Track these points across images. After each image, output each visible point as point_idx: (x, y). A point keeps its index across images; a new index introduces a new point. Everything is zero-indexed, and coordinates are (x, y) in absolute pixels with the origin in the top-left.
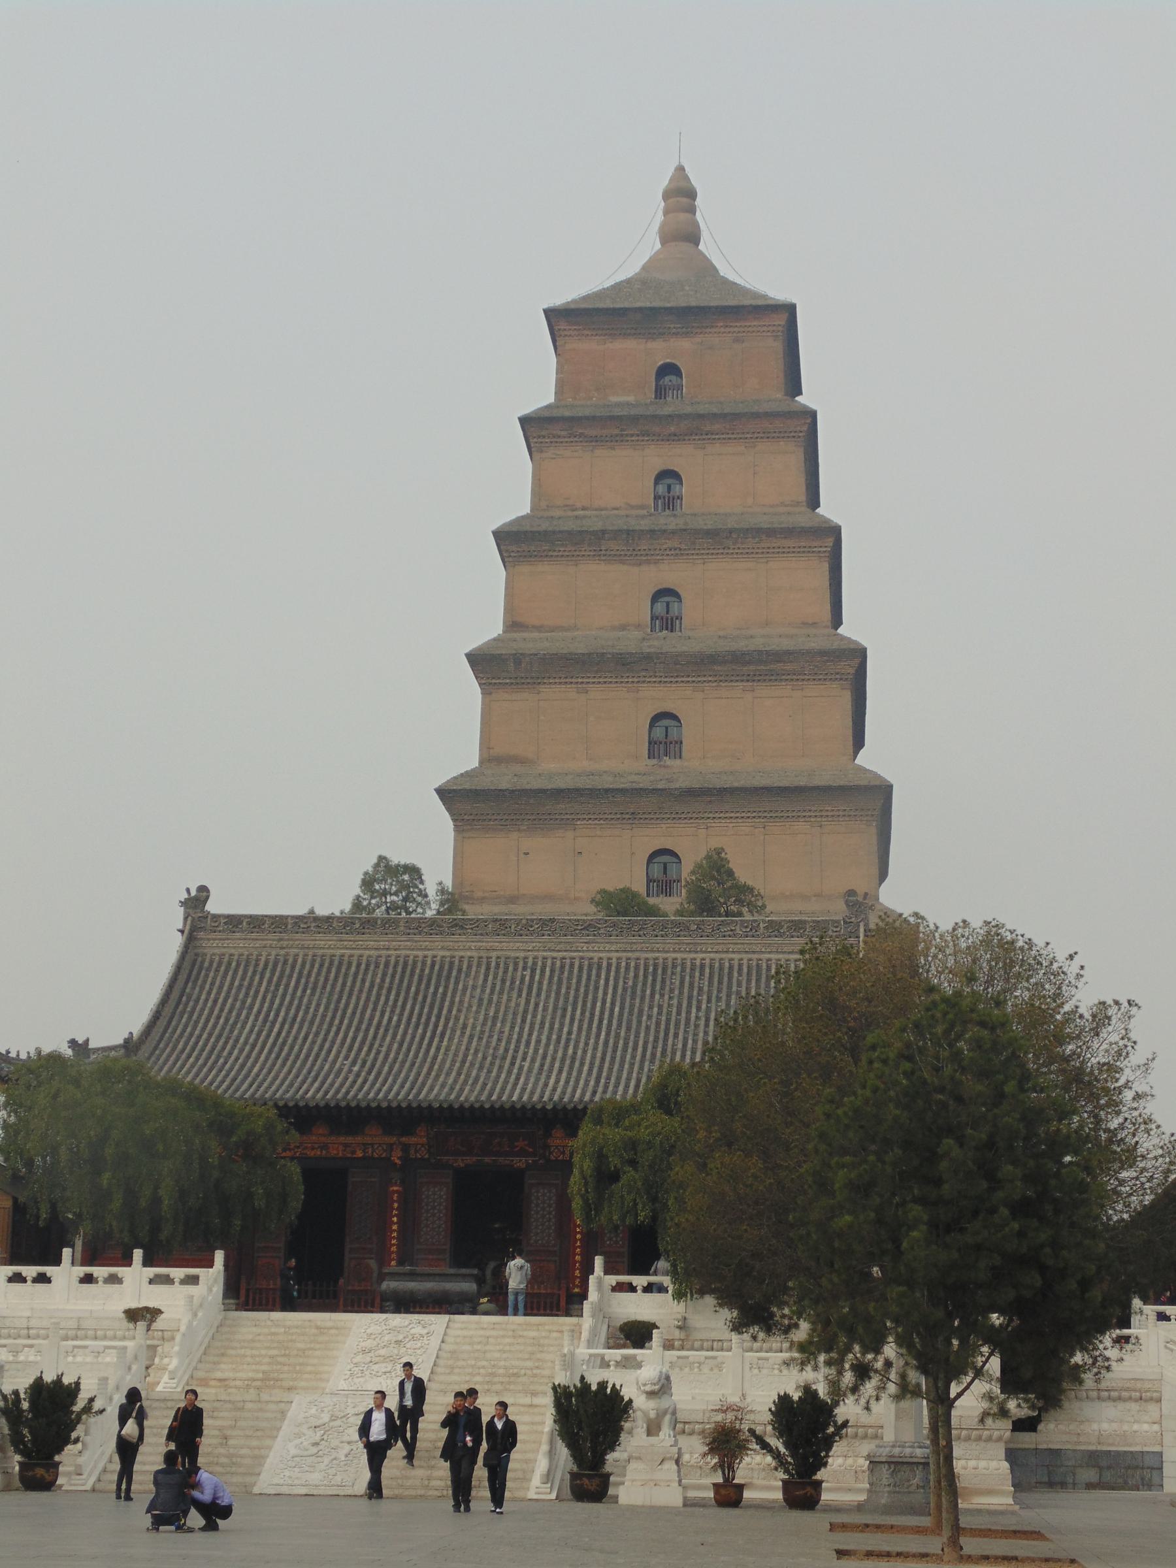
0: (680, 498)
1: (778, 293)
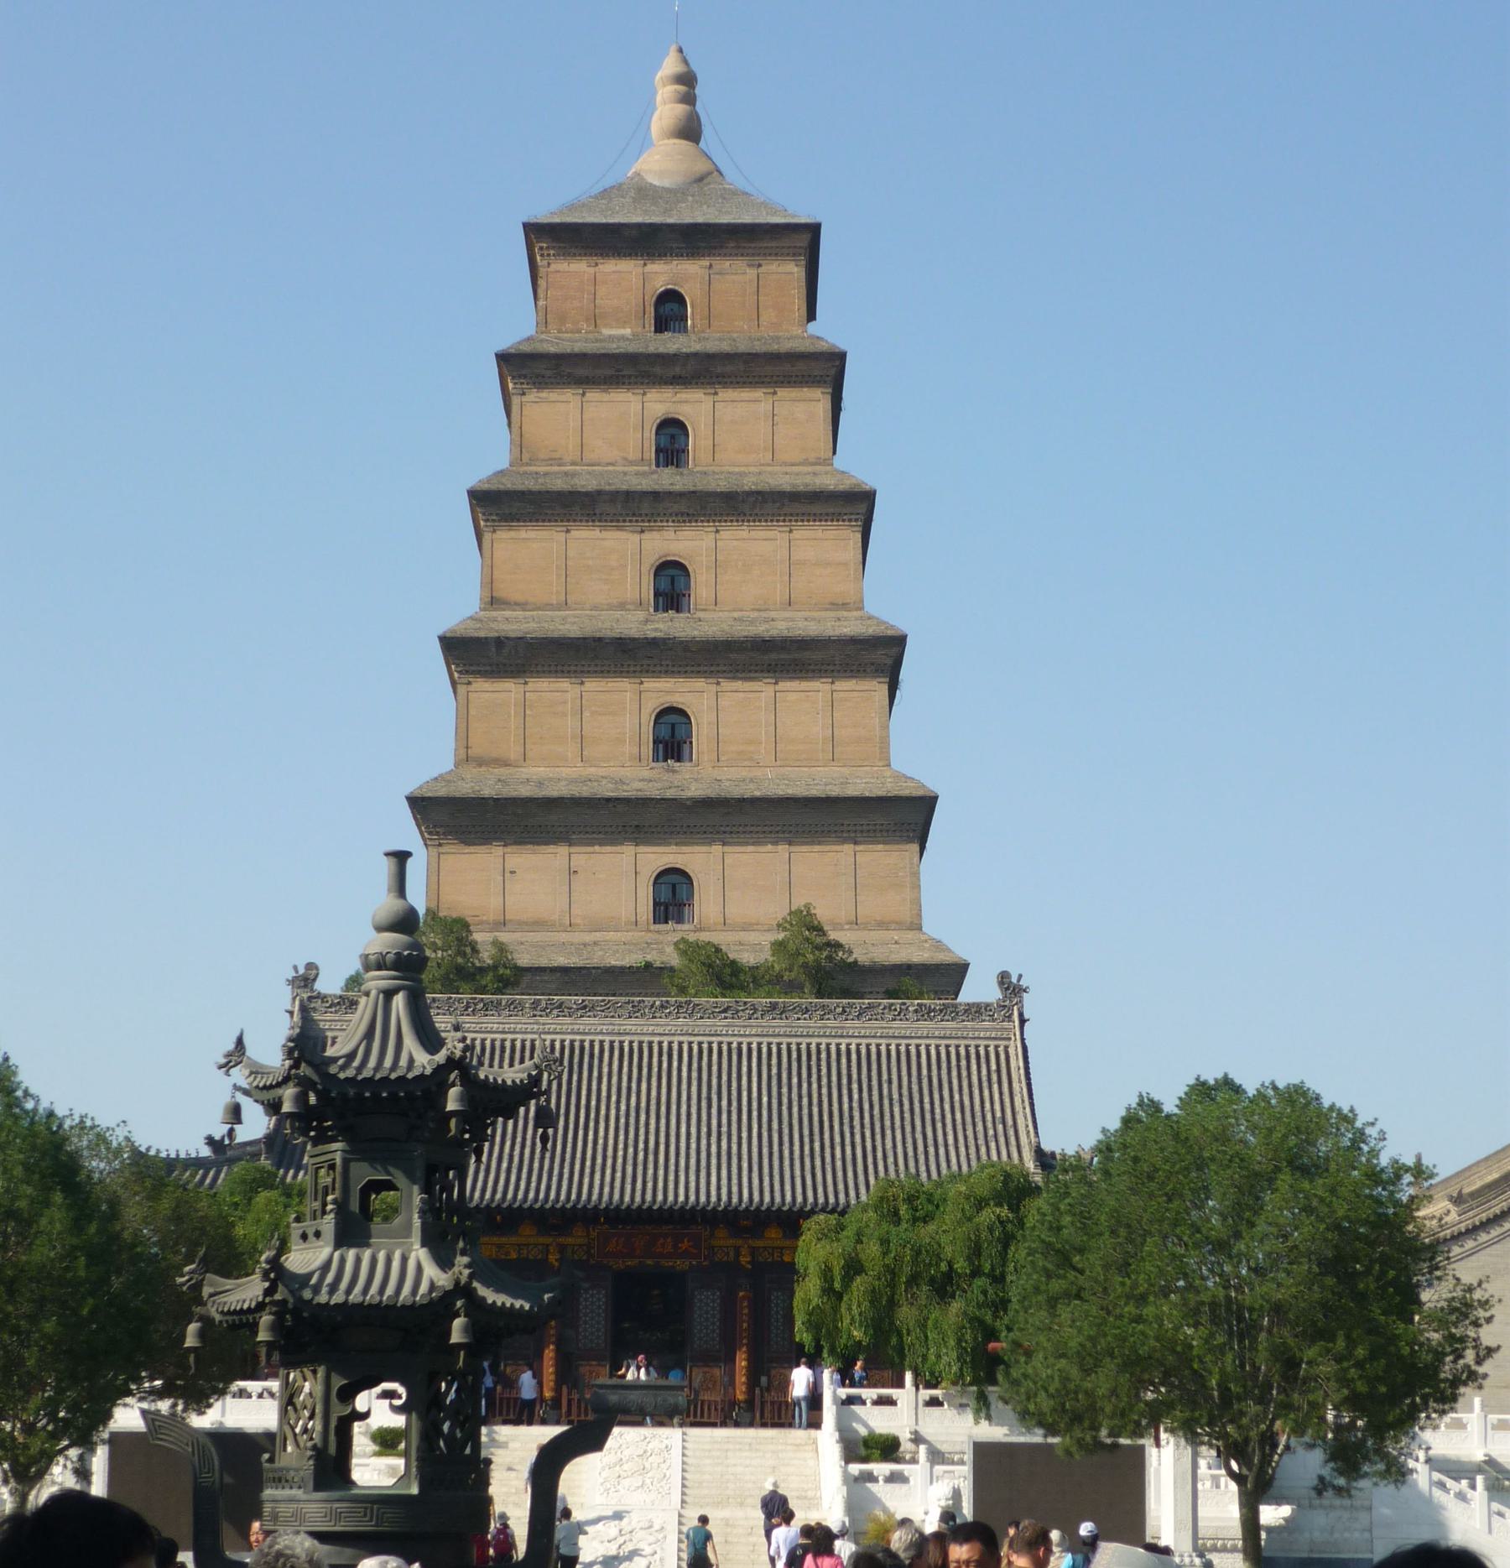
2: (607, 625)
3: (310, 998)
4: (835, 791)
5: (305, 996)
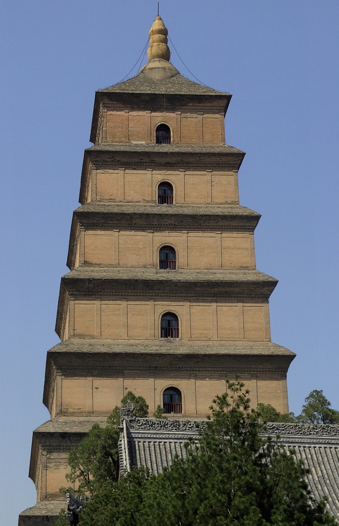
4: (248, 352)
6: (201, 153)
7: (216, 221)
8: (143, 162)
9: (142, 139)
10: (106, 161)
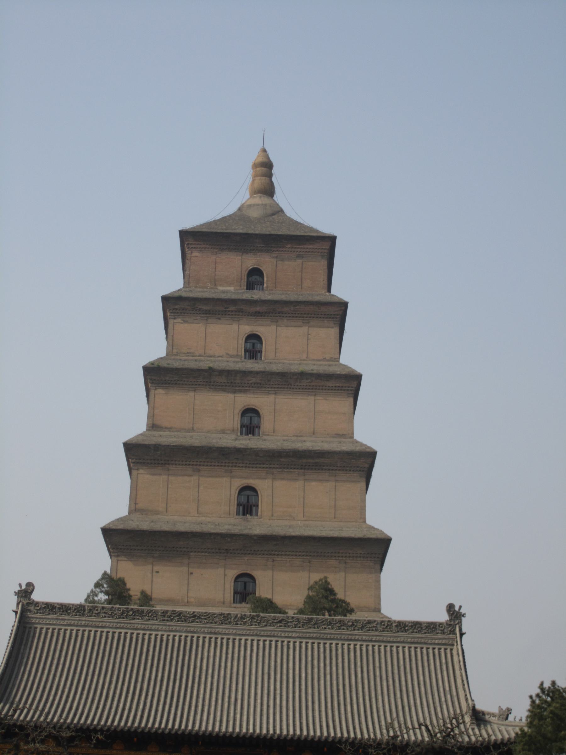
0: (261, 352)
1: (325, 229)
2: (214, 441)
3: (28, 604)
4: (336, 534)
5: (25, 602)
6: (297, 302)
7: (309, 380)
8: (229, 311)
9: (230, 285)
10: (186, 310)
